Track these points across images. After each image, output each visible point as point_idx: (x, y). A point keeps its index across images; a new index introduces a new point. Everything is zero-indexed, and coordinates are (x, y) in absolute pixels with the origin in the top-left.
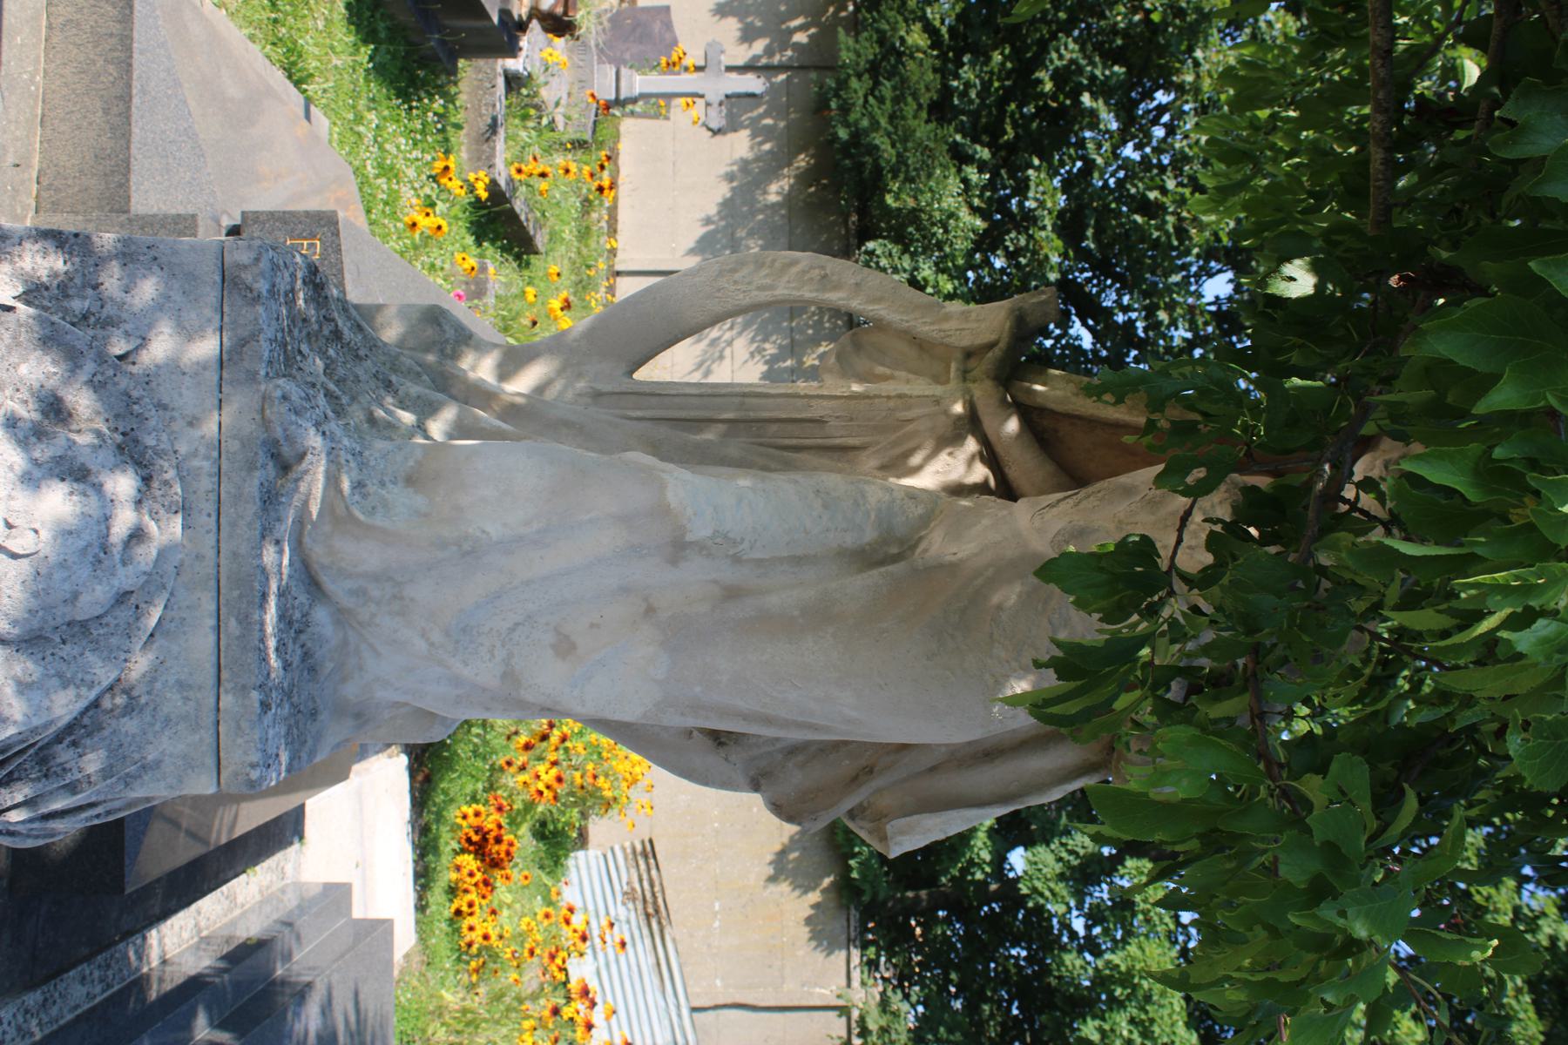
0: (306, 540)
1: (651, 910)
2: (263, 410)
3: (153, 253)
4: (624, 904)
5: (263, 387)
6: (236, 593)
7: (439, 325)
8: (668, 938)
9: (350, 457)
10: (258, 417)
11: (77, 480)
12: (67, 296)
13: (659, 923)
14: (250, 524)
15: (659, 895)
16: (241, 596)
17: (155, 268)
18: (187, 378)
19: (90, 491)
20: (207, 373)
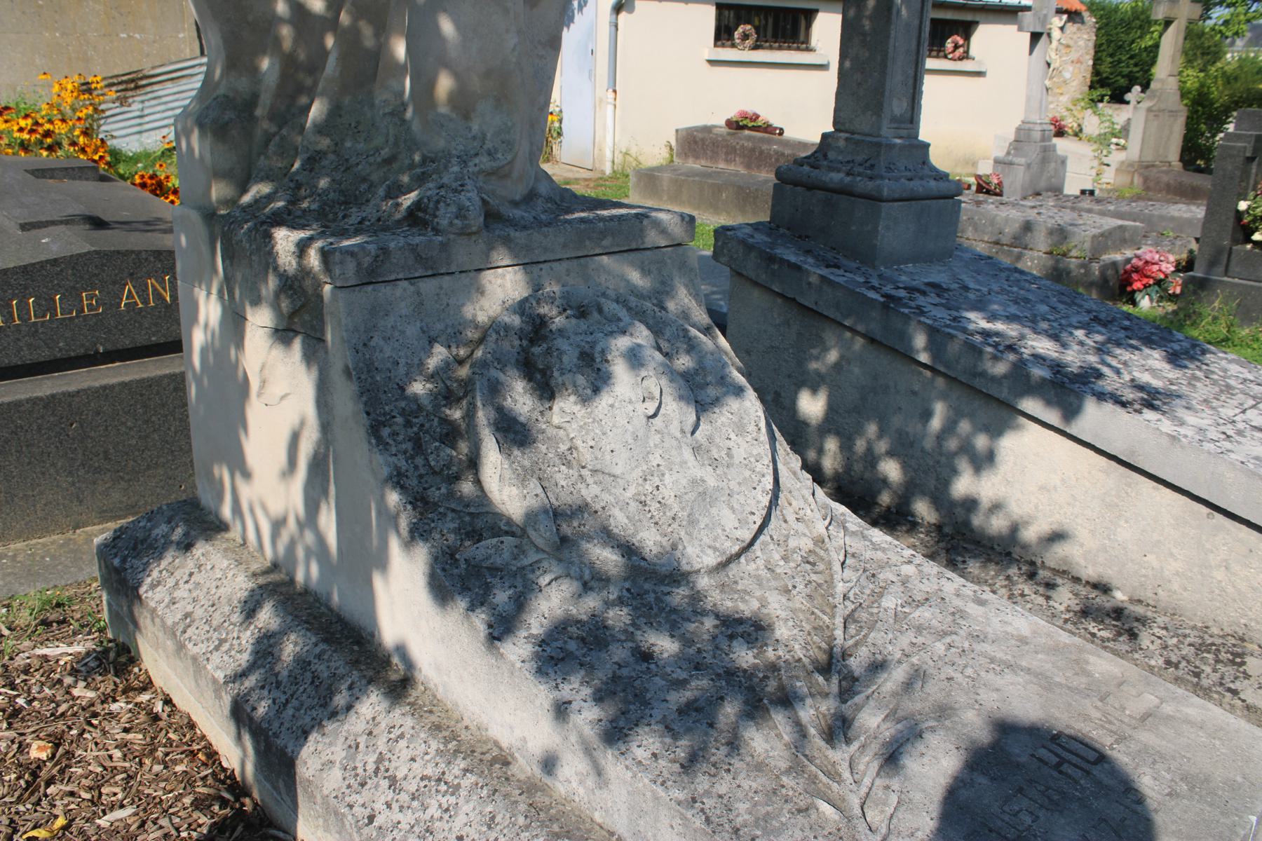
0: (518, 198)
1: (132, 85)
2: (470, 234)
3: (360, 347)
4: (130, 105)
5: (452, 237)
6: (587, 243)
7: (227, 124)
8: (152, 72)
9: (471, 164)
10: (474, 238)
11: (593, 360)
12: (420, 408)
13: (141, 79)
14: (546, 237)
15: (120, 79)
16: (589, 238)
17: (372, 343)
18: (450, 302)
19: (598, 348)
20: (445, 285)
